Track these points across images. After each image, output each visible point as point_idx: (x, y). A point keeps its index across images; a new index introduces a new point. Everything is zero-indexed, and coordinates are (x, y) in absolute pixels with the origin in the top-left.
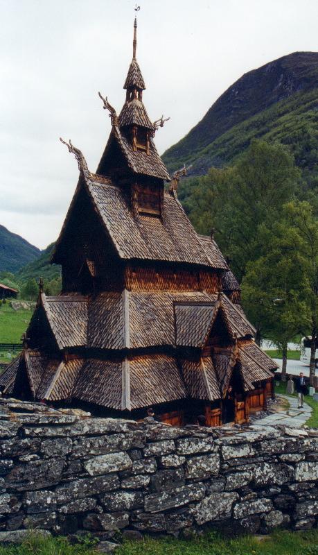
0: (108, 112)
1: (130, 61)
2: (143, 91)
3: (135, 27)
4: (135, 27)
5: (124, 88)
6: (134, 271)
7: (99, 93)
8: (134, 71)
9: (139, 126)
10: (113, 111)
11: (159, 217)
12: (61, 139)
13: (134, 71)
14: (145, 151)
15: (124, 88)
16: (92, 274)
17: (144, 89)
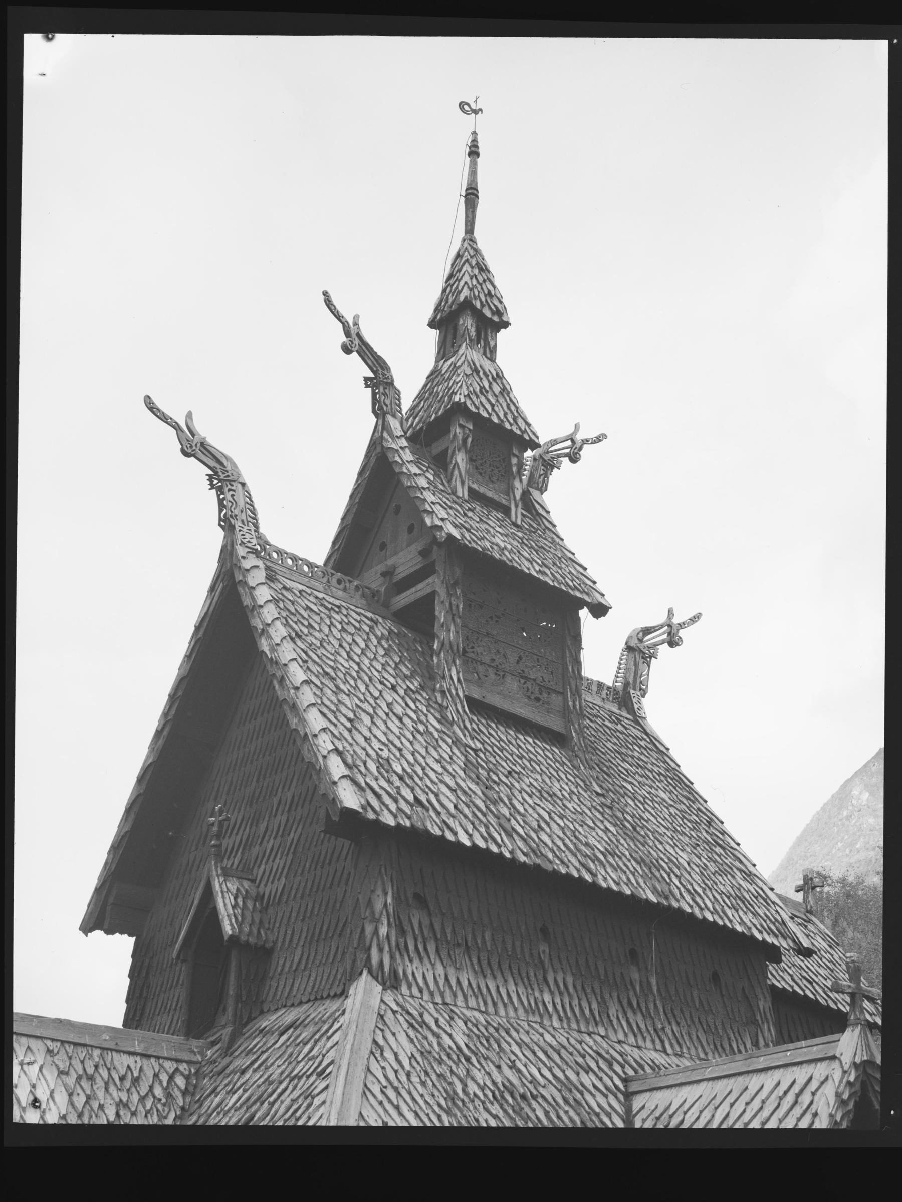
0: (360, 369)
3: (474, 152)
4: (474, 152)
5: (432, 324)
6: (421, 901)
7: (325, 293)
9: (476, 418)
11: (558, 739)
12: (151, 406)
15: (432, 324)
16: (228, 929)
17: (506, 325)
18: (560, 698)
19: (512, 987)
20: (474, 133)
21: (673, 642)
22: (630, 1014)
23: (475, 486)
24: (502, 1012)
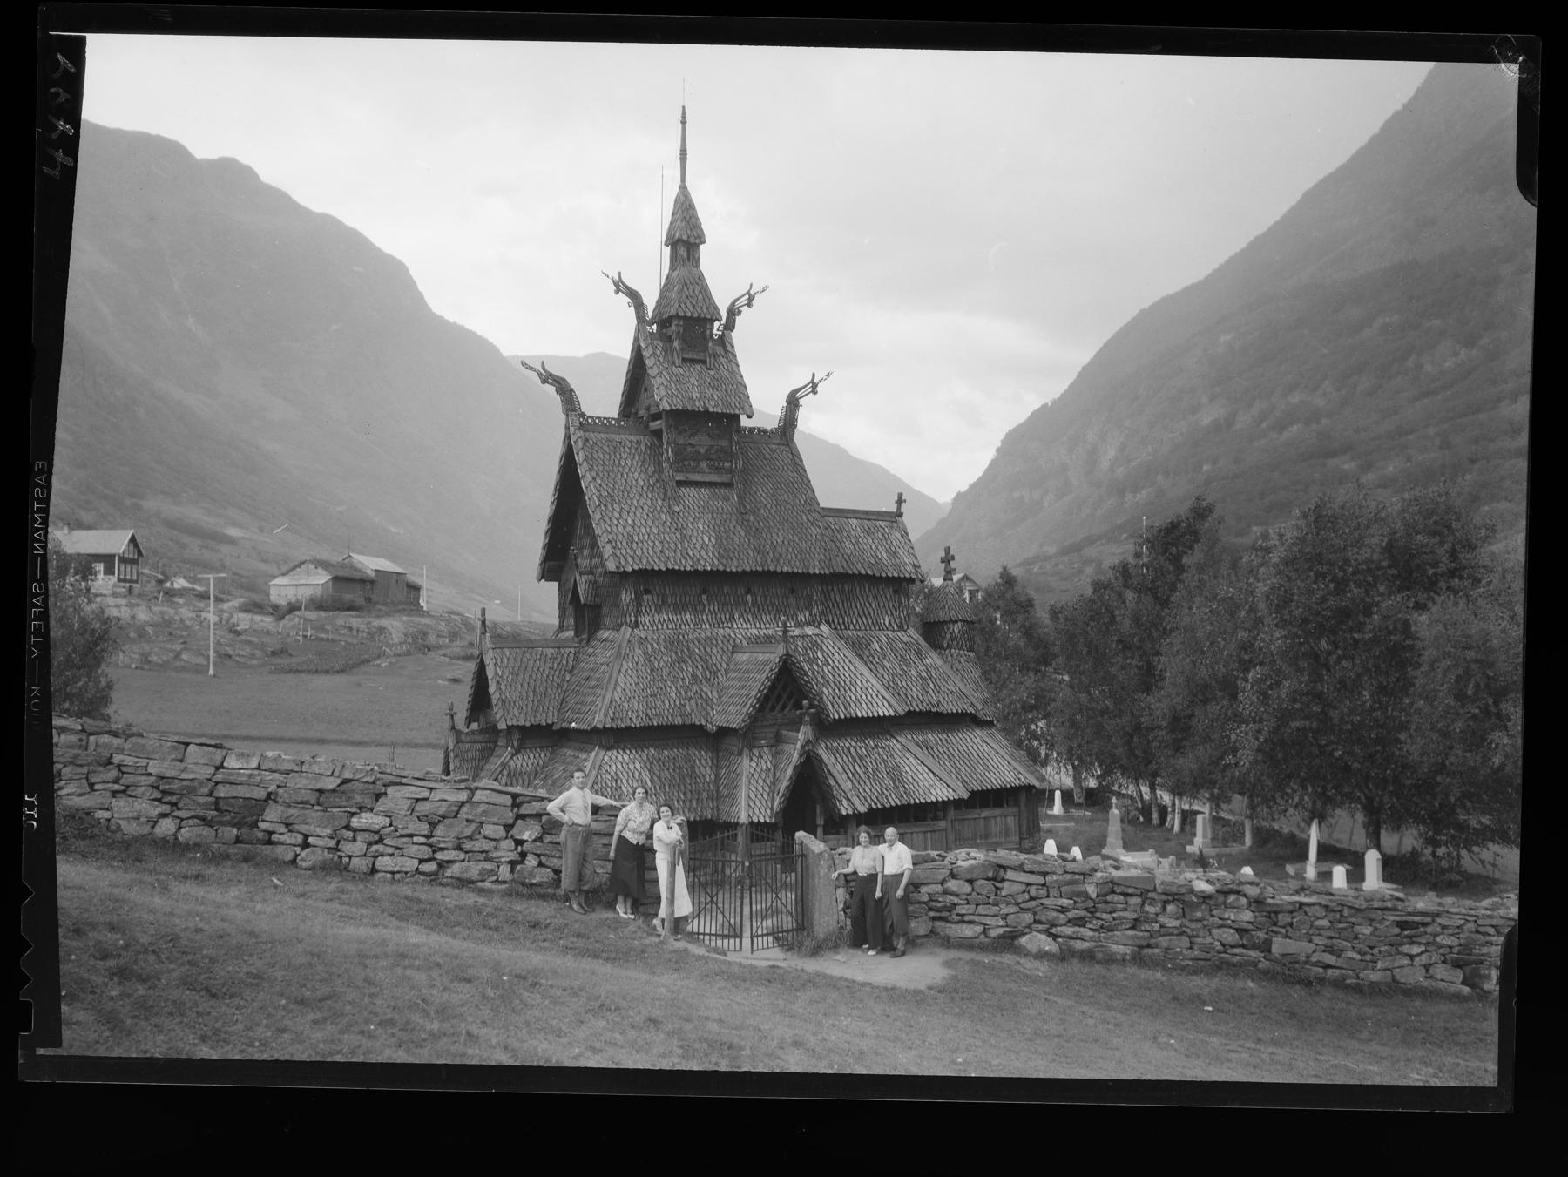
0: (624, 299)
1: (673, 192)
2: (702, 247)
3: (684, 122)
4: (684, 122)
5: (666, 245)
6: (647, 592)
8: (685, 210)
9: (685, 318)
10: (635, 297)
13: (685, 210)
14: (704, 362)
16: (582, 601)
17: (704, 242)
18: (729, 464)
19: (688, 616)
20: (684, 108)
21: (815, 392)
22: (745, 615)
23: (686, 356)
24: (683, 627)
